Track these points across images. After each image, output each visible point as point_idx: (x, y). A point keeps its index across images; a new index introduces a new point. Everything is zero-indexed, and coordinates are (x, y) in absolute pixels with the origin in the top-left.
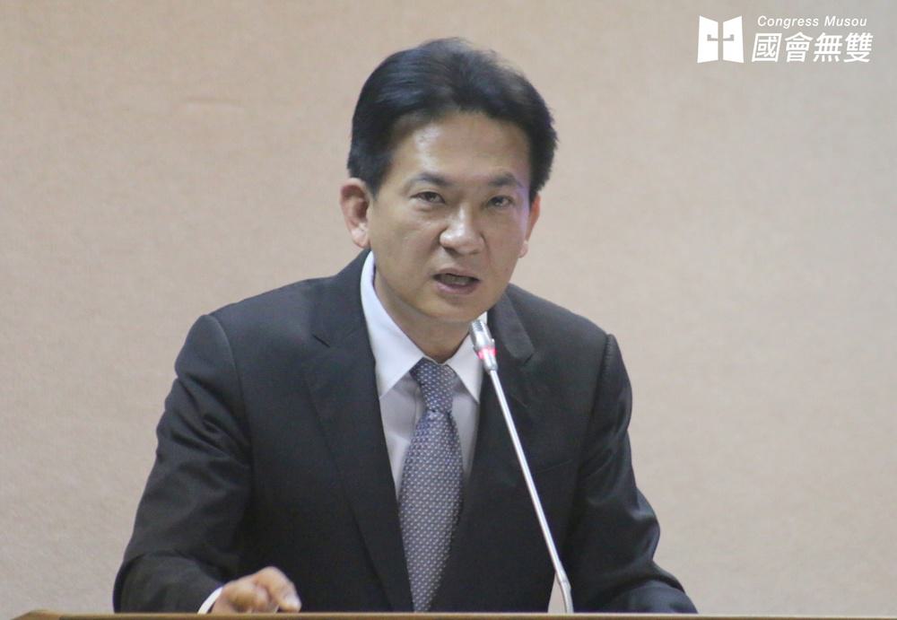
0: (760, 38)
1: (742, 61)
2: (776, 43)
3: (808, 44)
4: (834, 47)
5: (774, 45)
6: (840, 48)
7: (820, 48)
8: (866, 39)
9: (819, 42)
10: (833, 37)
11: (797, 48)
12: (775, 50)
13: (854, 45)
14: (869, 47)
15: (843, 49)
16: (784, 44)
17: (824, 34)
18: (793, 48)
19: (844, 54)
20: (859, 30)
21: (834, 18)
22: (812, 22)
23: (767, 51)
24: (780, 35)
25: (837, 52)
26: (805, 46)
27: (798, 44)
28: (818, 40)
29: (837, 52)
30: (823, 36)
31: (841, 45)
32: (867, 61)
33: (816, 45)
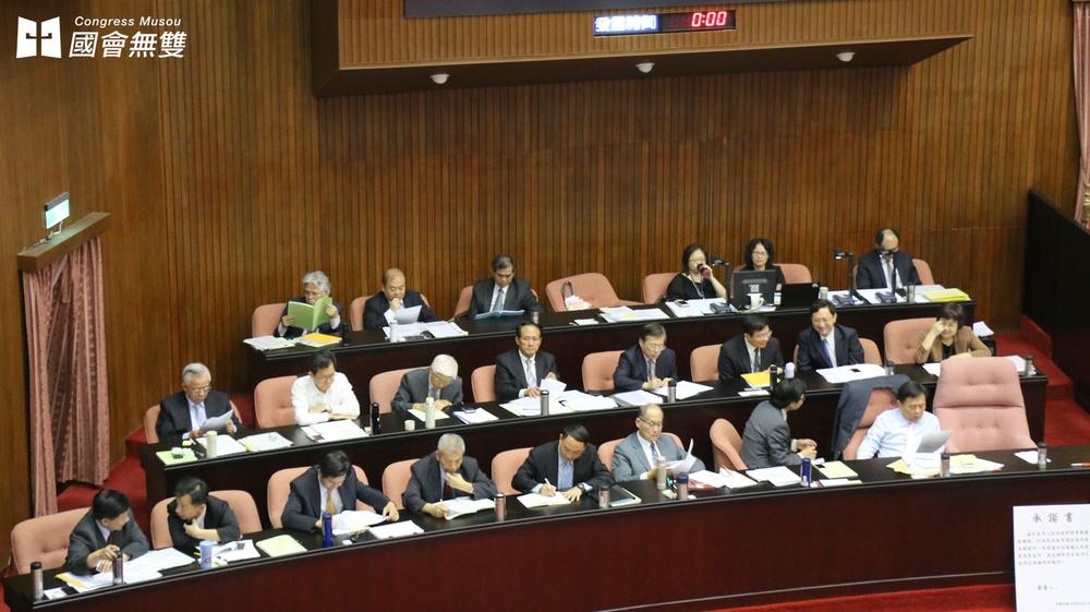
0: (77, 36)
3: (124, 41)
6: (154, 46)
10: (148, 36)
13: (168, 43)
15: (158, 45)
16: (100, 41)
18: (109, 45)
24: (97, 34)
25: (151, 48)
27: (114, 41)
29: (151, 48)
30: (138, 34)
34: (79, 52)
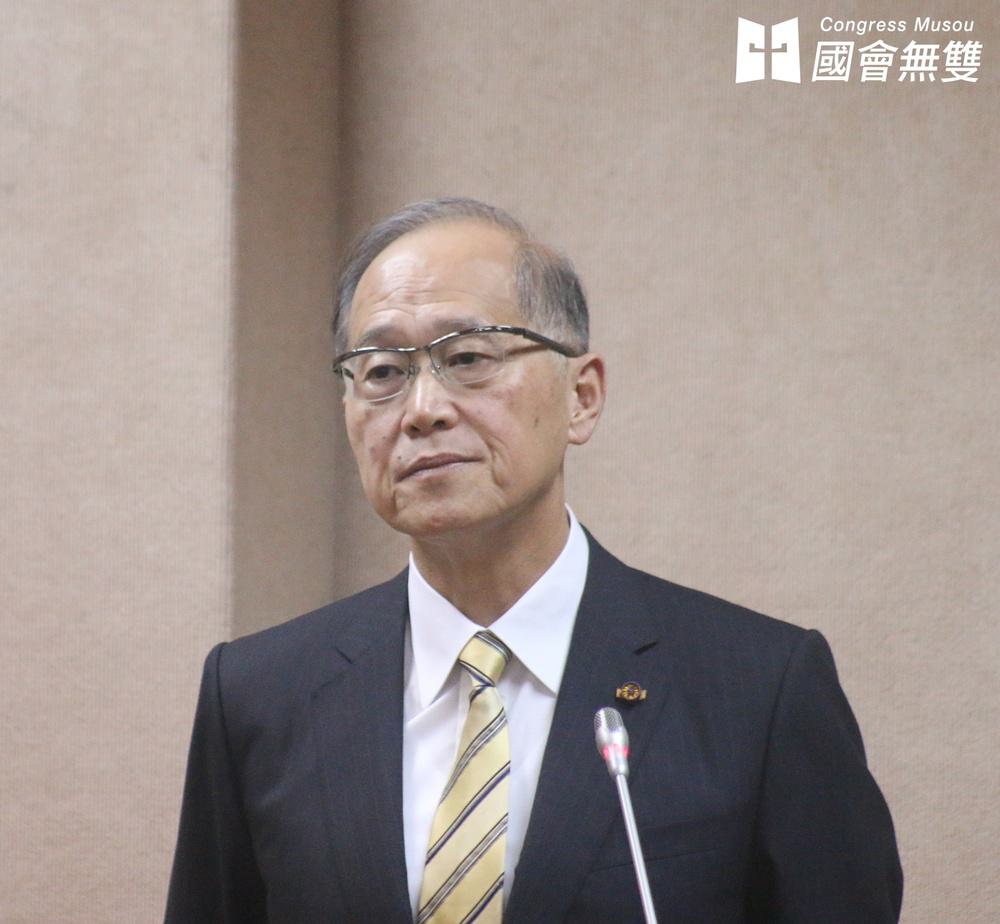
0: (823, 48)
1: (798, 81)
2: (846, 55)
3: (891, 56)
4: (927, 62)
5: (844, 58)
6: (936, 63)
7: (909, 63)
8: (973, 49)
9: (907, 54)
10: (926, 47)
11: (876, 62)
12: (845, 64)
13: (956, 58)
14: (976, 61)
15: (941, 63)
16: (857, 56)
17: (913, 42)
18: (870, 62)
19: (942, 71)
20: (963, 37)
21: (928, 19)
22: (897, 26)
23: (833, 67)
24: (852, 44)
25: (932, 68)
26: (887, 59)
27: (877, 56)
28: (905, 51)
29: (932, 68)
30: (912, 45)
31: (937, 58)
32: (974, 80)
33: (903, 58)
34: (826, 74)
